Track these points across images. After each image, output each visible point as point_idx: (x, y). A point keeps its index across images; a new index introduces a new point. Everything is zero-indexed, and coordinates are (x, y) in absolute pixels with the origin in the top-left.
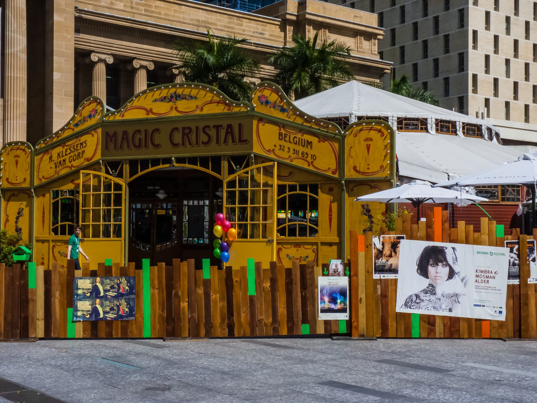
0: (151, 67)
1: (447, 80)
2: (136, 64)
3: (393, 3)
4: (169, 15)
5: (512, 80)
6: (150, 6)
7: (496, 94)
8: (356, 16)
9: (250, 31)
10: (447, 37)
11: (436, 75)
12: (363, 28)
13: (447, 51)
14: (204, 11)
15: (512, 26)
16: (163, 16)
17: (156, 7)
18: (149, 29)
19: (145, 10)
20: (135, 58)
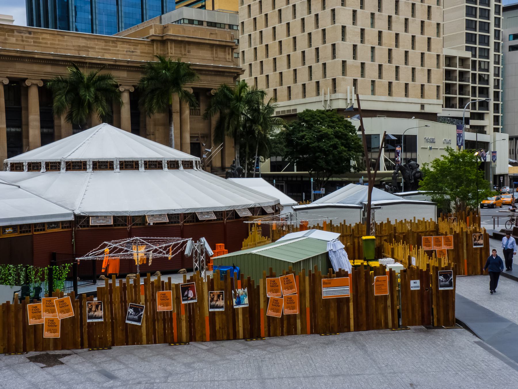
0: (41, 84)
1: (324, 65)
2: (28, 83)
3: (288, 2)
4: (54, 44)
5: (377, 63)
6: (38, 38)
7: (363, 75)
8: (212, 34)
9: (124, 51)
10: (324, 31)
11: (318, 61)
12: (217, 43)
13: (324, 42)
14: (84, 39)
15: (376, 21)
16: (49, 45)
17: (43, 39)
18: (36, 56)
19: (34, 42)
20: (27, 79)
